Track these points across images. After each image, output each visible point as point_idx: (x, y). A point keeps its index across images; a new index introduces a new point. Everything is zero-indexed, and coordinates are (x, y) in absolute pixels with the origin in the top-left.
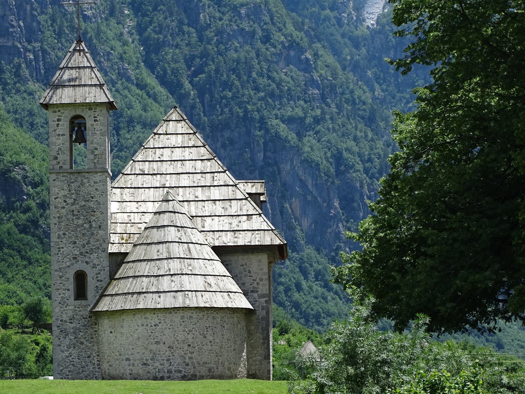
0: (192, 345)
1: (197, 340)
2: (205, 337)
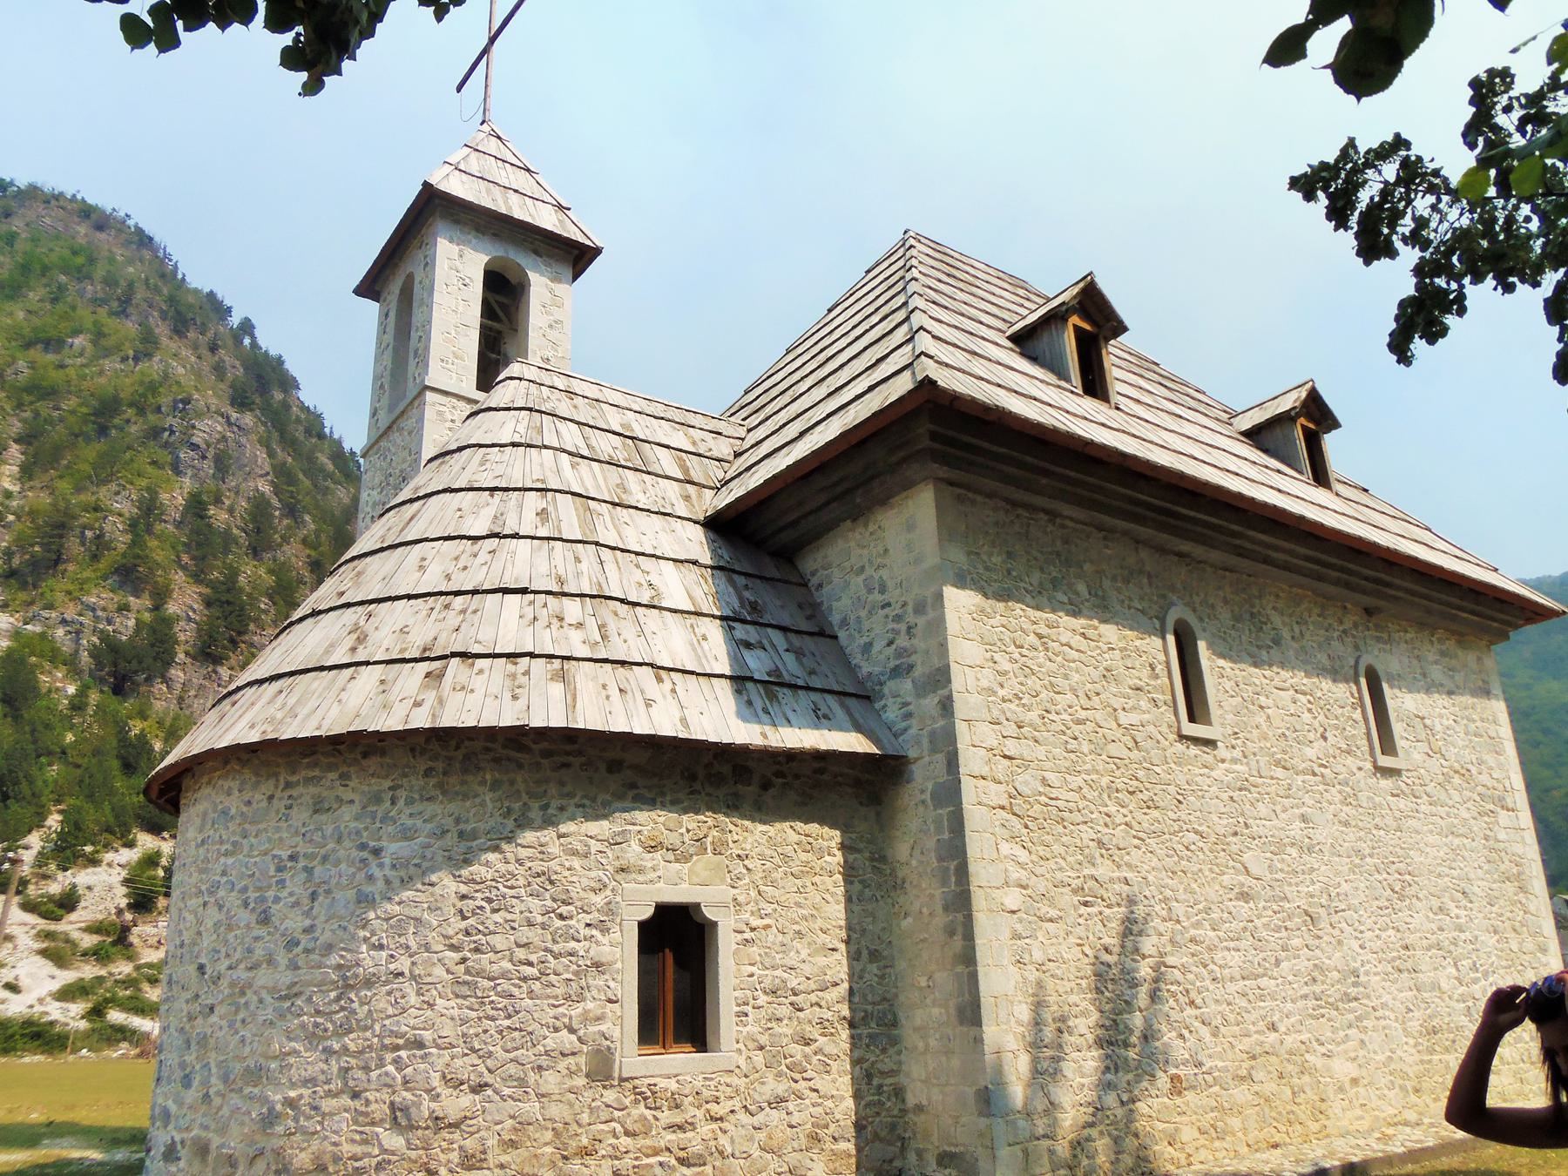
0: (209, 970)
1: (231, 936)
2: (265, 920)
